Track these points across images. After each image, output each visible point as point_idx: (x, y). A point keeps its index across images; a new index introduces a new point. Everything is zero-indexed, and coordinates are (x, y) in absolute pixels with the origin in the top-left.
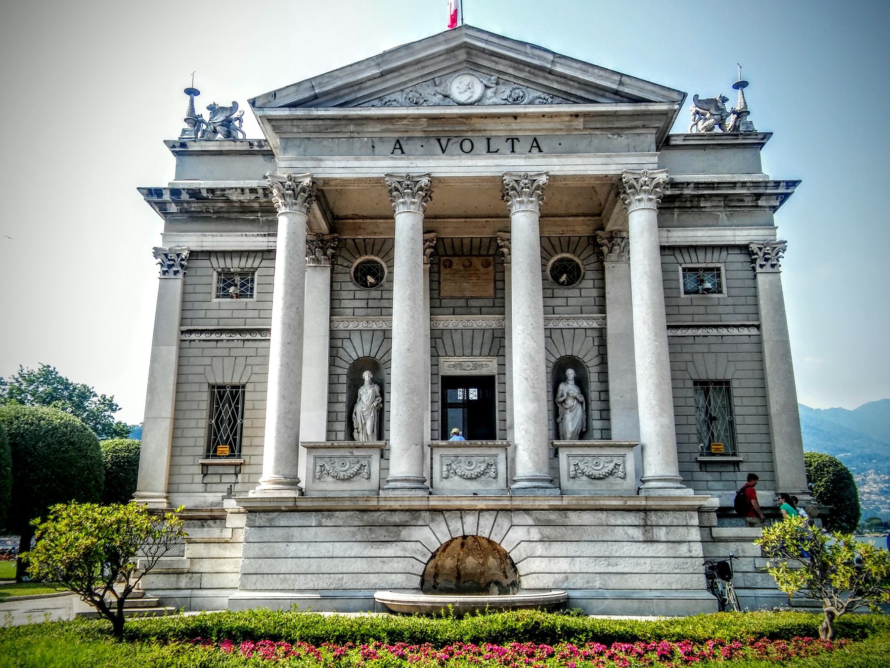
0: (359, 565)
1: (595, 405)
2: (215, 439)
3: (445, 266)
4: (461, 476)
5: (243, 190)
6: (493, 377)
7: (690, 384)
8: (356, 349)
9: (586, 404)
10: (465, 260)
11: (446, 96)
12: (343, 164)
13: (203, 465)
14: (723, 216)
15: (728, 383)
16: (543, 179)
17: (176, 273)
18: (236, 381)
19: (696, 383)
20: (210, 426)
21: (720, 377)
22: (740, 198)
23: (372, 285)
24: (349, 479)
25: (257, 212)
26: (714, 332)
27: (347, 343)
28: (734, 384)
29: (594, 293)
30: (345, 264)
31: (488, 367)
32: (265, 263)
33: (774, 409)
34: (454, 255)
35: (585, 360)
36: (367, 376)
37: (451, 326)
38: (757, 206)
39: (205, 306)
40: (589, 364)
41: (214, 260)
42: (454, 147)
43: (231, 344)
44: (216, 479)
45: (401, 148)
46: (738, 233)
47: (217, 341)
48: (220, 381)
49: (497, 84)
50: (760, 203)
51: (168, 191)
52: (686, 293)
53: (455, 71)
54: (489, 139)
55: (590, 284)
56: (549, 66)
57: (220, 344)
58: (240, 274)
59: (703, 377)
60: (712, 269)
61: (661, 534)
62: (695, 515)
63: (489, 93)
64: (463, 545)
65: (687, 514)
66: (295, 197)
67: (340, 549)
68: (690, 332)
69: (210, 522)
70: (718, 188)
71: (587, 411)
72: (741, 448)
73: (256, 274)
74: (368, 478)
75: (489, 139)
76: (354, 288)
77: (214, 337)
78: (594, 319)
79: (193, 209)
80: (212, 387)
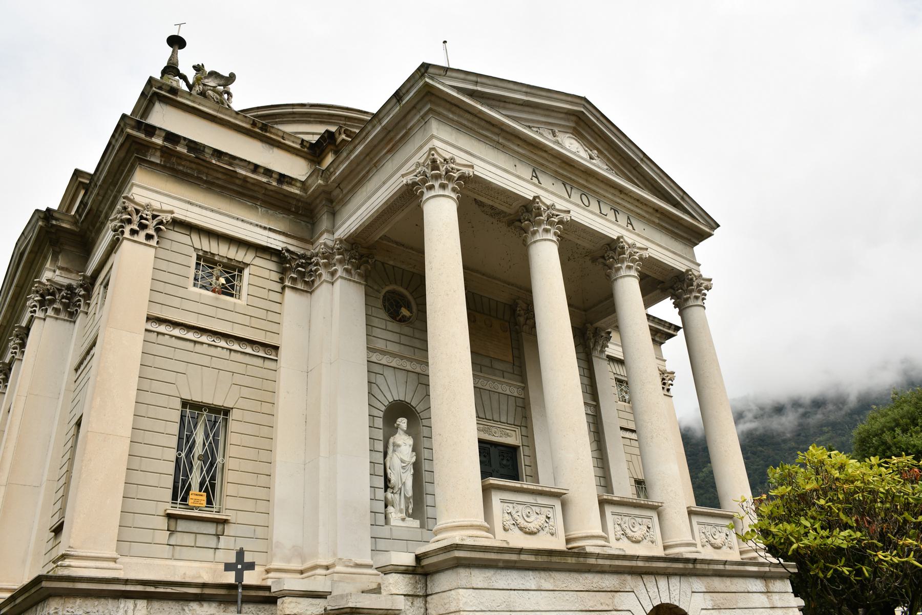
2: (184, 482)
5: (256, 168)
8: (395, 390)
13: (170, 516)
17: (149, 237)
18: (218, 402)
20: (178, 460)
30: (376, 288)
32: (259, 261)
36: (403, 422)
39: (181, 292)
41: (195, 237)
43: (212, 351)
44: (188, 539)
47: (195, 342)
48: (197, 398)
51: (164, 134)
57: (198, 348)
58: (225, 266)
73: (246, 272)
76: (388, 318)
77: (191, 335)
79: (181, 168)
80: (185, 404)
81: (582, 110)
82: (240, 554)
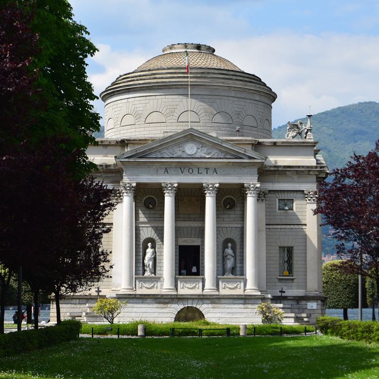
0: (155, 315)
1: (238, 258)
3: (181, 200)
4: (188, 288)
6: (199, 246)
7: (278, 248)
9: (235, 257)
10: (190, 200)
11: (183, 152)
12: (147, 177)
14: (295, 177)
15: (292, 247)
16: (217, 185)
19: (280, 247)
21: (289, 245)
22: (303, 171)
23: (151, 208)
24: (150, 288)
25: (101, 173)
26: (289, 227)
27: (141, 232)
28: (295, 248)
29: (240, 213)
30: (140, 199)
31: (195, 242)
33: (308, 258)
34: (185, 196)
35: (235, 240)
36: (149, 245)
37: (183, 226)
38: (309, 174)
40: (237, 241)
42: (186, 171)
45: (167, 171)
46: (301, 185)
49: (202, 147)
50: (311, 173)
52: (279, 209)
53: (187, 141)
54: (198, 169)
55: (238, 209)
56: (220, 144)
59: (283, 245)
60: (290, 200)
61: (250, 306)
62: (260, 300)
63: (199, 150)
64: (187, 309)
65: (258, 300)
66: (129, 190)
67: (149, 310)
68: (279, 227)
69: (90, 300)
70: (293, 168)
71: (235, 260)
72: (295, 273)
74: (157, 288)
75: (198, 169)
78: (239, 223)
81: (191, 133)
82: (98, 288)
